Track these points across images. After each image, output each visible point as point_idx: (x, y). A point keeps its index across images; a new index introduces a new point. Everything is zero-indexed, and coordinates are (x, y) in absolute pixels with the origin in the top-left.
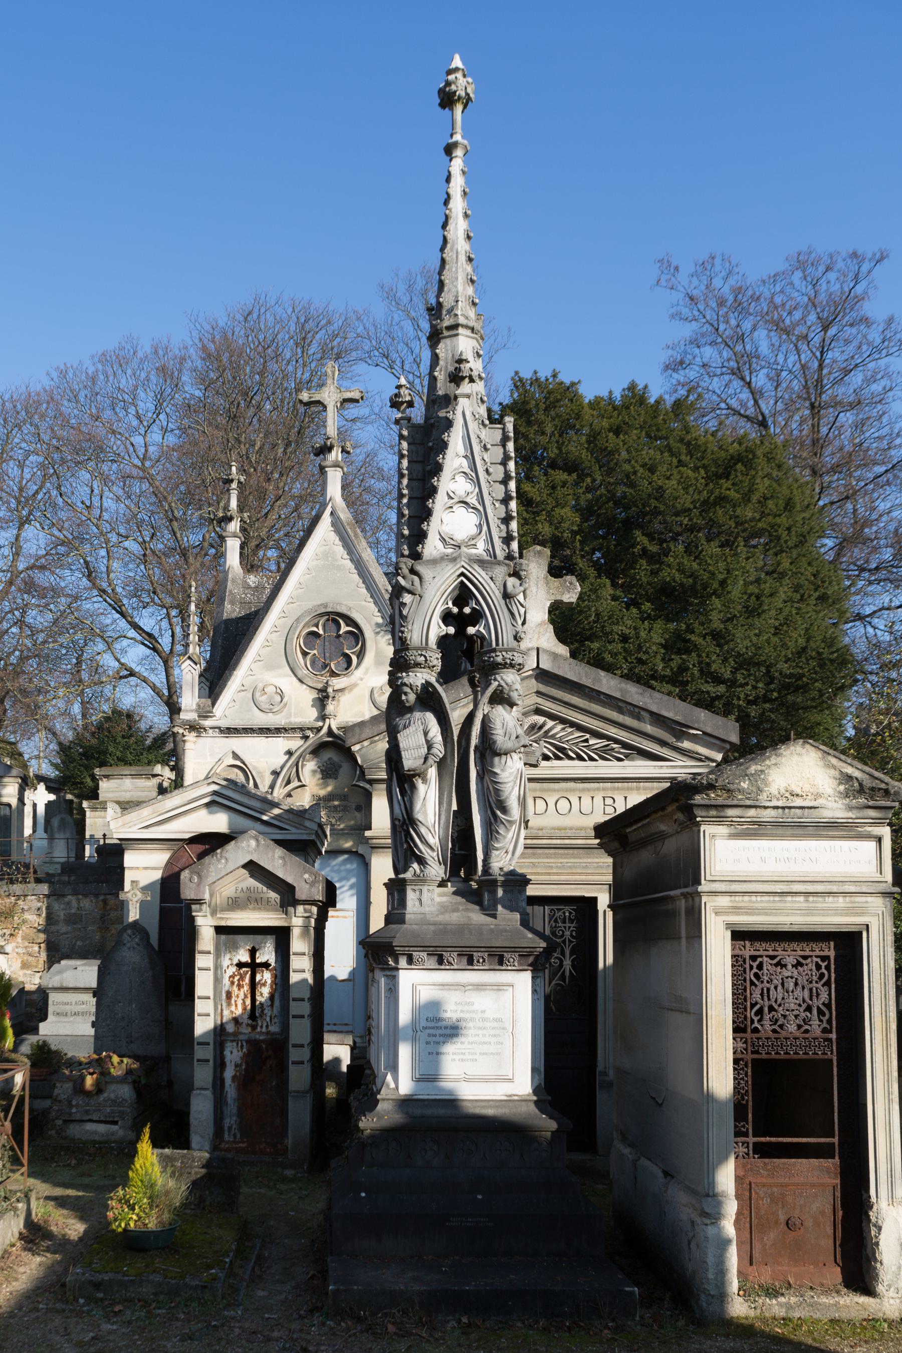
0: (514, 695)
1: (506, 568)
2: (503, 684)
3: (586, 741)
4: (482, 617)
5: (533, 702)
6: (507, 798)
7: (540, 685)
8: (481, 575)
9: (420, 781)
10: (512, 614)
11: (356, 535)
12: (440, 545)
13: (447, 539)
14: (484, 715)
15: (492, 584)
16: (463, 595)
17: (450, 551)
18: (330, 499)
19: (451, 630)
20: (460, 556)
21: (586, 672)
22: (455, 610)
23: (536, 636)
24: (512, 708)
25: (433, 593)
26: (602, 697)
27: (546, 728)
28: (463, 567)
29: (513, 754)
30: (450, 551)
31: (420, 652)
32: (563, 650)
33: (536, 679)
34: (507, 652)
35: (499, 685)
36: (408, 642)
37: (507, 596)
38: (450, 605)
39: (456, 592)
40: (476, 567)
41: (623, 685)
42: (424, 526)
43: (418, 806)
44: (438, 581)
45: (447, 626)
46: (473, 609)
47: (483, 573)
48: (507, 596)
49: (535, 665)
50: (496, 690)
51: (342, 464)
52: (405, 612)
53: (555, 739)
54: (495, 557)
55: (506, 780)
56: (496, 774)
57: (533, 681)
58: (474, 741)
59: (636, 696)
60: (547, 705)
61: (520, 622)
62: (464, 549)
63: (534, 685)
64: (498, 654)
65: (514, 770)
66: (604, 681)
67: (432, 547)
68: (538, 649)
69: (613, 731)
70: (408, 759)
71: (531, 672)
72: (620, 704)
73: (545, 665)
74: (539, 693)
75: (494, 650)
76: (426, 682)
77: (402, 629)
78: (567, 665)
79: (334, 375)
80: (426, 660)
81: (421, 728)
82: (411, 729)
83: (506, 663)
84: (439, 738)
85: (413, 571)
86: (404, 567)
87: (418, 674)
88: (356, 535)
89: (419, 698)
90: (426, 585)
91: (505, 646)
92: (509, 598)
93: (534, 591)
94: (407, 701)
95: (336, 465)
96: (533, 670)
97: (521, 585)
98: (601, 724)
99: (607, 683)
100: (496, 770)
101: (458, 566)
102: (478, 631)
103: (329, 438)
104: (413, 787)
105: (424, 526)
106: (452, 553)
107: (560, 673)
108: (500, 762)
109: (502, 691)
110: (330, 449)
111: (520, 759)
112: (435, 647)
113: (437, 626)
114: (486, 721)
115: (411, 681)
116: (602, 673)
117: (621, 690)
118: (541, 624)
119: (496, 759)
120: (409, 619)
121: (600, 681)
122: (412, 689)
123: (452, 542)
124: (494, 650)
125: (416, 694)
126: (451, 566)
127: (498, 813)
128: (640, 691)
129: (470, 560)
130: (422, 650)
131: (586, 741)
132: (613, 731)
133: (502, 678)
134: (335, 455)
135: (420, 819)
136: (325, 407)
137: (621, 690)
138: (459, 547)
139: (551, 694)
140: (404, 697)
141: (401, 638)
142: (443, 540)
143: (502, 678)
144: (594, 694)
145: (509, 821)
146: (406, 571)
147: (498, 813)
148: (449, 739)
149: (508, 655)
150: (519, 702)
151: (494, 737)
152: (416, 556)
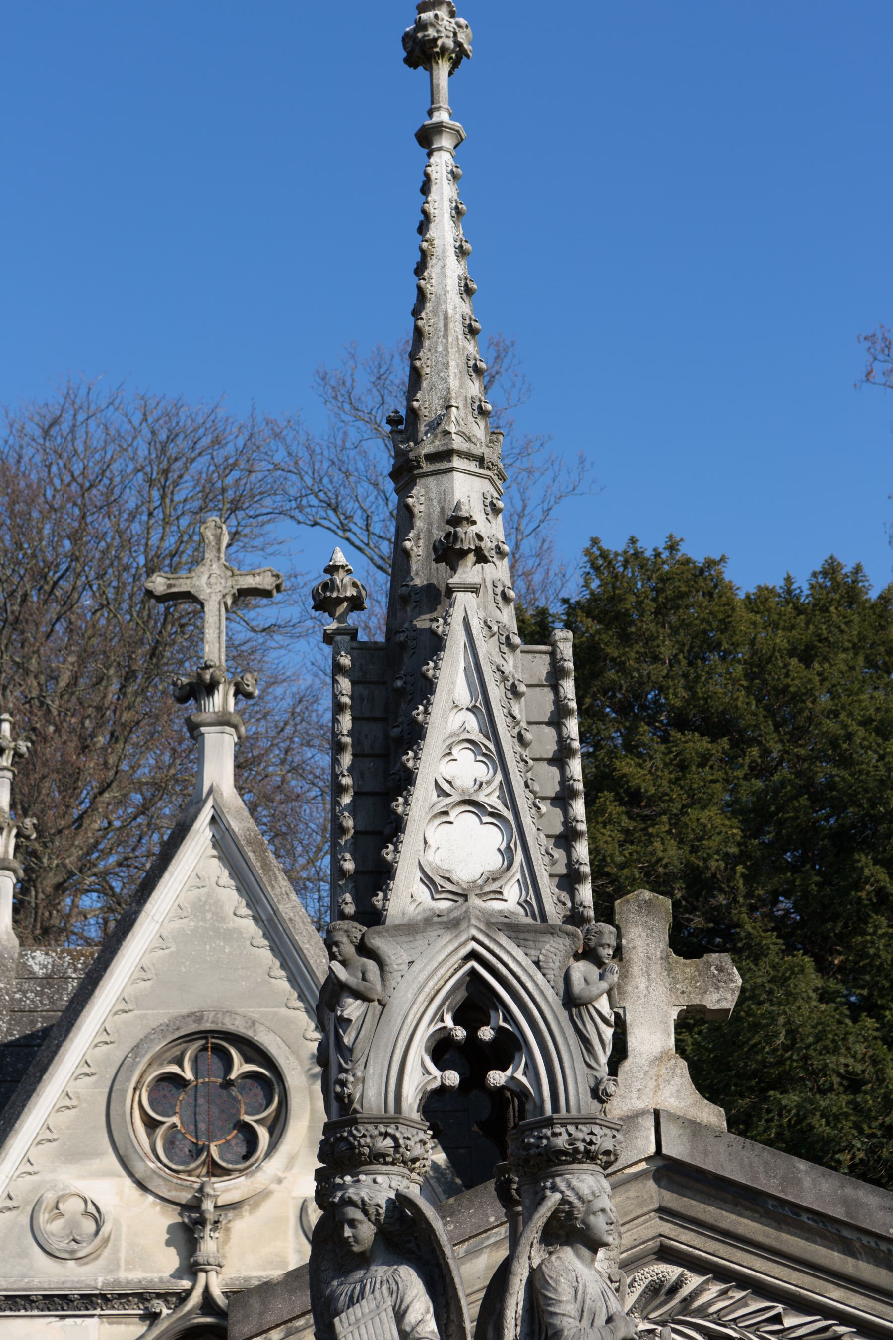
0: (599, 1223)
1: (567, 942)
2: (573, 1198)
3: (777, 1319)
4: (519, 1048)
5: (652, 1233)
7: (667, 1195)
8: (514, 957)
10: (585, 1041)
11: (266, 865)
12: (423, 893)
13: (438, 880)
14: (532, 1271)
15: (539, 977)
16: (475, 999)
17: (444, 905)
18: (211, 791)
19: (453, 1078)
20: (466, 915)
21: (766, 1164)
22: (460, 1033)
23: (652, 1084)
24: (595, 1252)
25: (410, 996)
26: (804, 1218)
27: (685, 1291)
28: (474, 939)
30: (444, 905)
31: (382, 1129)
32: (712, 1115)
33: (657, 1181)
35: (564, 1201)
36: (356, 1105)
37: (572, 1002)
38: (449, 1022)
39: (462, 995)
40: (503, 939)
41: (849, 1191)
42: (388, 853)
44: (421, 971)
45: (442, 1068)
46: (500, 1031)
47: (519, 953)
48: (572, 1002)
49: (652, 1149)
50: (556, 1212)
51: (236, 719)
52: (347, 1040)
53: (706, 1317)
54: (544, 918)
57: (651, 1184)
59: (880, 1215)
60: (686, 1240)
61: (603, 1059)
62: (475, 901)
63: (652, 1192)
64: (557, 1130)
66: (807, 1182)
67: (407, 896)
68: (657, 1114)
69: (834, 1296)
71: (643, 1166)
72: (846, 1233)
73: (676, 1147)
74: (664, 1212)
75: (549, 1122)
76: (399, 1195)
77: (343, 1076)
78: (723, 1149)
80: (397, 1147)
81: (389, 1302)
82: (367, 1305)
83: (576, 1151)
85: (364, 950)
86: (345, 940)
87: (379, 1179)
88: (266, 865)
89: (383, 1233)
90: (394, 980)
91: (574, 1112)
92: (578, 1006)
93: (642, 986)
94: (357, 1241)
95: (223, 721)
96: (648, 1159)
97: (602, 977)
98: (807, 1280)
99: (813, 1186)
101: (464, 938)
102: (512, 1078)
103: (207, 667)
105: (388, 853)
106: (450, 911)
107: (709, 1165)
109: (570, 1215)
110: (211, 688)
112: (416, 1116)
113: (420, 1069)
114: (537, 1284)
115: (364, 1193)
116: (802, 1165)
117: (846, 1202)
118: (659, 1059)
120: (357, 1053)
121: (798, 1182)
122: (366, 1213)
123: (449, 887)
124: (549, 1122)
125: (376, 1223)
126: (447, 937)
128: (887, 1203)
129: (489, 924)
131: (777, 1319)
132: (834, 1296)
133: (569, 1185)
134: (222, 700)
137: (846, 1202)
138: (465, 897)
139: (691, 1214)
140: (348, 1232)
141: (339, 1097)
142: (428, 881)
143: (569, 1185)
144: (787, 1211)
146: (349, 949)
148: (453, 1328)
149: (582, 1133)
150: (610, 1239)
151: (556, 1321)
152: (372, 917)
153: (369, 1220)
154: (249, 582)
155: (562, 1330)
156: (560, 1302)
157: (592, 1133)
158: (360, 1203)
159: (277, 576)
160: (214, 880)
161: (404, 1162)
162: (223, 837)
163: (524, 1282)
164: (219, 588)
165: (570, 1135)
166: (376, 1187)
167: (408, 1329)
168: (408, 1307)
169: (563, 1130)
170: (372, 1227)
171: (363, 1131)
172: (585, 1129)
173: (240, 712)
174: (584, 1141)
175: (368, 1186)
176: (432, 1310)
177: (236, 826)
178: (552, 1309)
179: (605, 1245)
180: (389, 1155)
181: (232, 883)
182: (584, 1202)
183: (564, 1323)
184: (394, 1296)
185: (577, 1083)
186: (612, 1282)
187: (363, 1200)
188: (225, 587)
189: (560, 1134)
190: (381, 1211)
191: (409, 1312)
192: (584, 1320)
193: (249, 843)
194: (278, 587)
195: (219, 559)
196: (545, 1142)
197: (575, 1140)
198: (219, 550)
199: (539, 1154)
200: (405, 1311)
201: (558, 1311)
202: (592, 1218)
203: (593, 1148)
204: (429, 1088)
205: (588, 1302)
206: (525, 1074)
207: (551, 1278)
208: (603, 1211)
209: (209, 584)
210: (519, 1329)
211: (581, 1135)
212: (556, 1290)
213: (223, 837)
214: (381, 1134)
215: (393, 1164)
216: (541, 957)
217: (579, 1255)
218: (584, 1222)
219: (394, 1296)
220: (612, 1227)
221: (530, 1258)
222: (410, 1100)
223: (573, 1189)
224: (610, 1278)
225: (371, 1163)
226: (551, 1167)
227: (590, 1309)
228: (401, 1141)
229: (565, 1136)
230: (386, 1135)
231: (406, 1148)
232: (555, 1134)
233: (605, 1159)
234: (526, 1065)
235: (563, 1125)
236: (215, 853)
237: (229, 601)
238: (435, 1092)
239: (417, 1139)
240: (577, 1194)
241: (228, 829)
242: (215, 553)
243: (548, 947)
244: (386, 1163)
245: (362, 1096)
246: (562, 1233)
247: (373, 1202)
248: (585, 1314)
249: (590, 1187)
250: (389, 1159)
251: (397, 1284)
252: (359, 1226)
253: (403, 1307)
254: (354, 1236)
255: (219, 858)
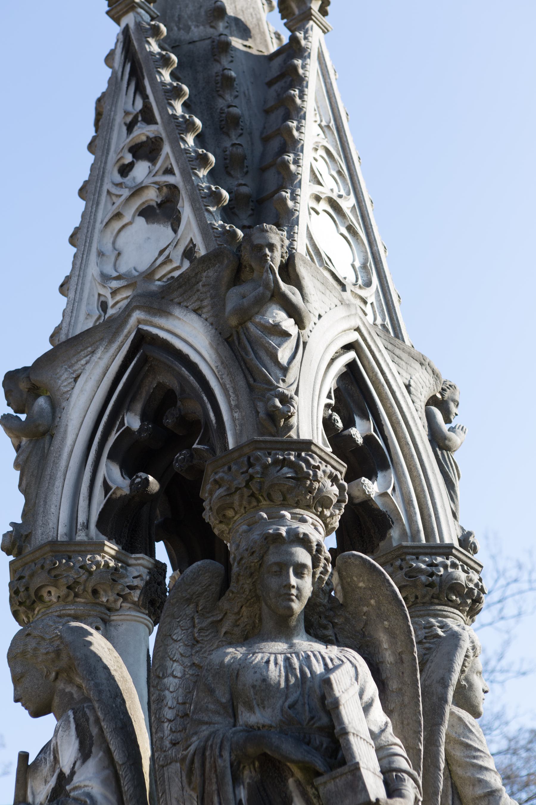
1: (432, 381)
4: (384, 466)
28: (358, 329)
178: (480, 762)
199: (431, 585)
216: (412, 383)
226: (432, 604)
232: (454, 565)
243: (417, 375)
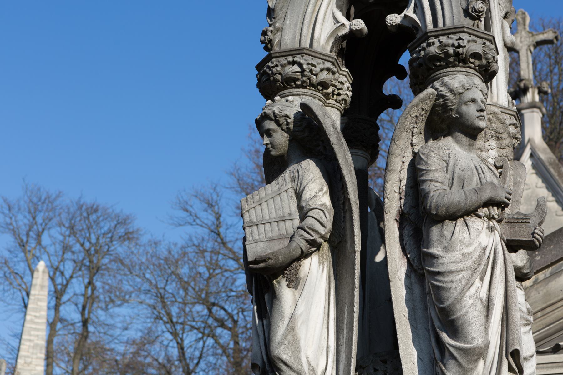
0: (471, 111)
2: (444, 91)
6: (457, 301)
9: (284, 283)
14: (415, 155)
18: (529, 141)
19: (359, 24)
29: (472, 220)
31: (290, 59)
34: (447, 35)
35: (440, 96)
43: (280, 331)
50: (434, 107)
51: (539, 104)
55: (453, 267)
56: (434, 257)
58: (393, 205)
64: (431, 41)
65: (474, 249)
70: (256, 242)
76: (303, 105)
79: (524, 19)
80: (303, 71)
83: (447, 54)
84: (326, 200)
87: (290, 98)
95: (533, 106)
100: (435, 250)
102: (406, 16)
103: (521, 80)
104: (274, 296)
108: (442, 235)
109: (445, 107)
111: (491, 229)
119: (435, 230)
122: (279, 124)
125: (288, 131)
127: (445, 336)
130: (294, 55)
133: (444, 85)
134: (532, 96)
135: (284, 357)
136: (517, 52)
145: (464, 351)
147: (445, 336)
149: (453, 40)
150: (482, 124)
153: (282, 129)
154: (541, 37)
155: (429, 192)
156: (430, 171)
157: (460, 39)
158: (272, 115)
159: (555, 32)
160: (534, 185)
161: (312, 85)
162: (537, 164)
163: (407, 164)
164: (526, 43)
165: (441, 42)
166: (288, 104)
167: (304, 204)
168: (304, 188)
169: (436, 41)
170: (286, 135)
171: (275, 63)
172: (455, 37)
173: (542, 100)
174: (453, 45)
175: (281, 104)
176: (326, 188)
177: (543, 156)
178: (423, 178)
179: (480, 130)
180: (298, 79)
181: (544, 185)
182: (455, 95)
183: (432, 187)
184: (296, 182)
185: (452, 7)
186: (497, 168)
187: (274, 113)
188: (529, 42)
189: (433, 43)
190: (289, 120)
191: (305, 191)
192: (453, 187)
193: (551, 164)
194: (556, 38)
195: (525, 29)
196: (422, 53)
197: (446, 46)
198: (524, 25)
199: (420, 65)
200: (303, 191)
201: (426, 178)
202: (464, 108)
203: (461, 50)
204: (340, 34)
205: (457, 171)
206: (415, 12)
207: (424, 154)
208: (474, 101)
209: (521, 42)
210: (403, 201)
211: (450, 42)
212: (426, 163)
213: (537, 164)
214: (289, 63)
215: (302, 86)
217: (457, 141)
218: (458, 112)
219: (296, 182)
220: (482, 114)
221: (412, 145)
222: (322, 42)
223: (445, 85)
224: (495, 166)
225: (285, 88)
227: (459, 177)
228: (305, 66)
229: (437, 44)
230: (294, 63)
231: (311, 71)
233: (477, 62)
234: (416, 5)
235: (437, 37)
236: (534, 171)
237: (532, 49)
238: (344, 37)
239: (322, 66)
240: (449, 88)
241: (539, 159)
242: (522, 26)
244: (297, 87)
245: (280, 41)
246: (444, 126)
247: (283, 113)
248: (455, 181)
249: (461, 81)
250: (299, 83)
251: (298, 172)
252: (274, 134)
253: (301, 189)
254: (271, 143)
255: (537, 174)
